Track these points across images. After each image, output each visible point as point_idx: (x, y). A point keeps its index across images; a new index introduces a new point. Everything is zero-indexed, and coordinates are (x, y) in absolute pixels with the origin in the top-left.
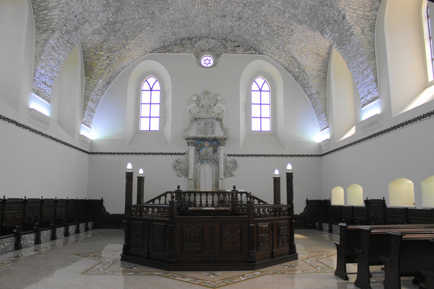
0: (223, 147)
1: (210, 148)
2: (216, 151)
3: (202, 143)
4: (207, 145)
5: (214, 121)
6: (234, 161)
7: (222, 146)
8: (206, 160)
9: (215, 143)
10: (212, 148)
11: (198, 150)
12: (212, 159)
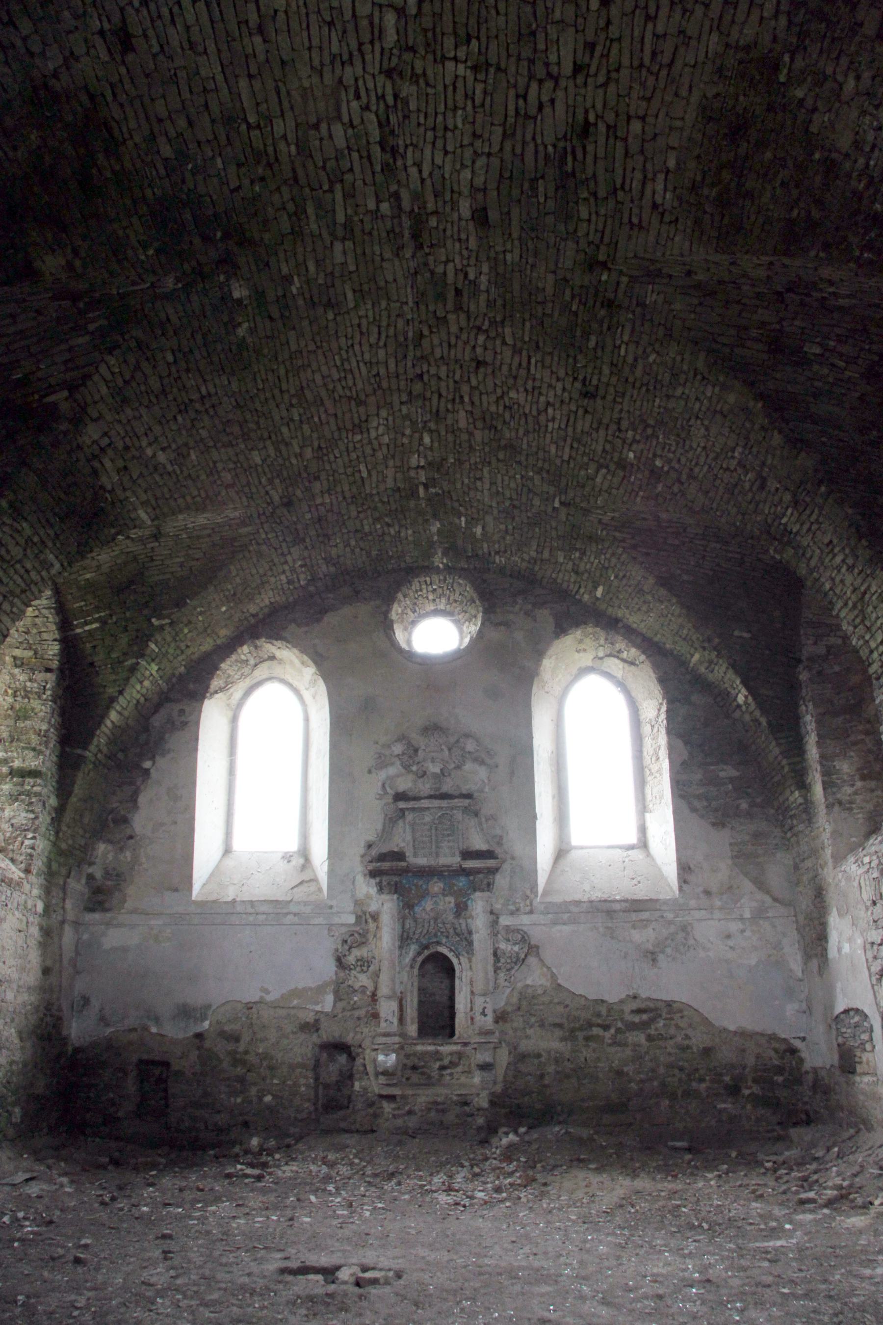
0: (487, 894)
1: (448, 899)
2: (466, 906)
3: (420, 883)
4: (436, 889)
7: (483, 891)
9: (462, 882)
12: (451, 931)
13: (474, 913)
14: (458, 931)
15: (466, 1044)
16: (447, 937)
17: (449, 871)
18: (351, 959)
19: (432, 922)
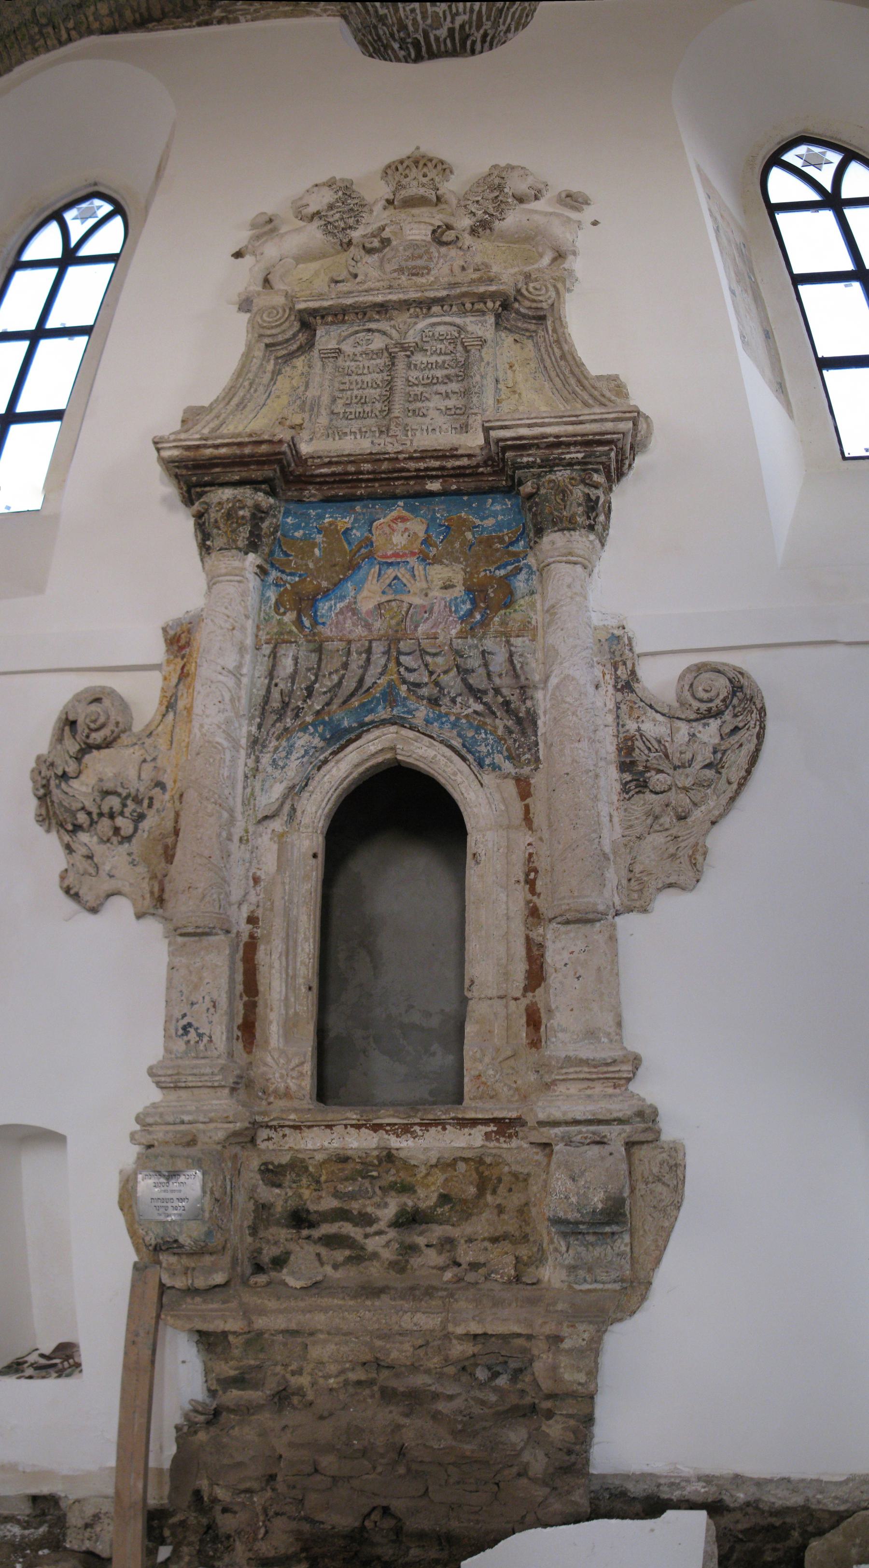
0: (581, 541)
1: (439, 573)
2: (508, 599)
4: (399, 540)
5: (481, 327)
6: (722, 685)
7: (570, 525)
8: (390, 696)
10: (455, 573)
11: (303, 602)
12: (452, 681)
13: (537, 618)
14: (478, 680)
15: (505, 1127)
16: (434, 702)
17: (443, 474)
18: (82, 789)
19: (378, 648)
